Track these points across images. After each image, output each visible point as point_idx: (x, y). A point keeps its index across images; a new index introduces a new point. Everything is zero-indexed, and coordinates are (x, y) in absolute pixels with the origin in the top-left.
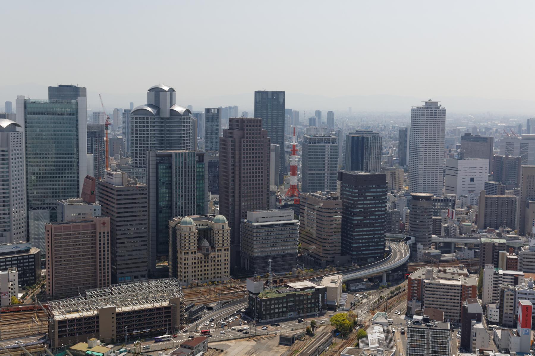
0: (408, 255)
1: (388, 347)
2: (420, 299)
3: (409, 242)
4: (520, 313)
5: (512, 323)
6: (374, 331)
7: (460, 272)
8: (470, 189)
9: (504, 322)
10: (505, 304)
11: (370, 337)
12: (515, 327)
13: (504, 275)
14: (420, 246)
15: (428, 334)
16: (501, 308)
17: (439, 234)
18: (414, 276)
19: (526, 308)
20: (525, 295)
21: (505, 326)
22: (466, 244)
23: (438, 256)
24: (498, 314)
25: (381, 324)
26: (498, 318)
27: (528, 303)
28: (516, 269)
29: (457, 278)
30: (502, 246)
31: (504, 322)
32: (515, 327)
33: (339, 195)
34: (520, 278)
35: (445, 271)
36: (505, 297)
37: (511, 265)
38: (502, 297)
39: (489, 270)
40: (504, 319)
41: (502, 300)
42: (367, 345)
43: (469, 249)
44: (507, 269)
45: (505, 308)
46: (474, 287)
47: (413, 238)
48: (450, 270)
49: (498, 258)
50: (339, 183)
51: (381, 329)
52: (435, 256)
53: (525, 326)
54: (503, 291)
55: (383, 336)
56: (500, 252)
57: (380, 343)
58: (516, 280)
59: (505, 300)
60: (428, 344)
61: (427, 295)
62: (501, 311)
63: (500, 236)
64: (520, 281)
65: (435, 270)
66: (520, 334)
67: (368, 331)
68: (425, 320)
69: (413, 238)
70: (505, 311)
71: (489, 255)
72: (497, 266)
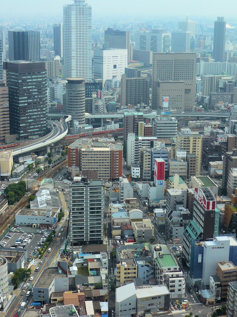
0: (67, 131)
1: (54, 206)
2: (79, 165)
3: (67, 120)
4: (156, 169)
5: (150, 178)
6: (41, 194)
7: (109, 140)
8: (114, 75)
9: (144, 178)
10: (144, 163)
11: (39, 199)
12: (153, 181)
13: (143, 140)
14: (76, 123)
15: (87, 191)
16: (141, 167)
17: (90, 111)
18: (72, 146)
19: (160, 165)
20: (159, 154)
21: (145, 180)
22: (112, 119)
23: (91, 130)
24: (139, 171)
25: (48, 189)
26: (139, 174)
27: (161, 160)
28: (151, 135)
29: (107, 146)
30: (140, 118)
31: (144, 178)
32: (153, 181)
33: (5, 82)
34: (155, 142)
35: (97, 141)
36: (145, 157)
37: (148, 132)
38: (142, 157)
39: (131, 138)
40: (144, 175)
41: (142, 160)
42: (37, 206)
43: (115, 122)
44: (145, 135)
45: (144, 166)
46: (120, 152)
47: (70, 116)
48: (101, 140)
49: (137, 128)
50: (5, 71)
51: (48, 192)
52: (88, 130)
53: (160, 178)
54: (142, 154)
55: (50, 197)
56: (140, 122)
57: (47, 204)
58: (152, 144)
59: (144, 160)
60: (87, 199)
61: (84, 161)
62: (142, 169)
63: (138, 110)
64: (154, 144)
65: (90, 140)
66: (156, 184)
67: (37, 194)
68: (83, 180)
69: (70, 116)
70: (144, 169)
71: (132, 125)
72: (137, 134)
